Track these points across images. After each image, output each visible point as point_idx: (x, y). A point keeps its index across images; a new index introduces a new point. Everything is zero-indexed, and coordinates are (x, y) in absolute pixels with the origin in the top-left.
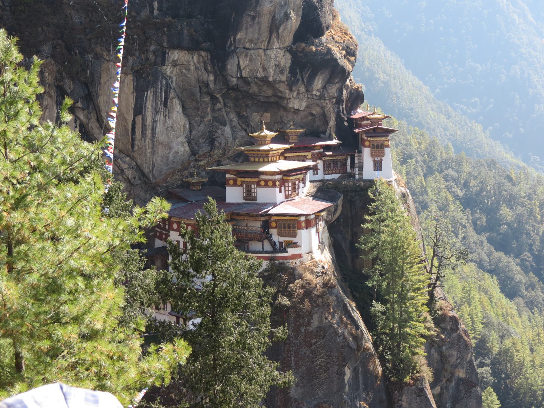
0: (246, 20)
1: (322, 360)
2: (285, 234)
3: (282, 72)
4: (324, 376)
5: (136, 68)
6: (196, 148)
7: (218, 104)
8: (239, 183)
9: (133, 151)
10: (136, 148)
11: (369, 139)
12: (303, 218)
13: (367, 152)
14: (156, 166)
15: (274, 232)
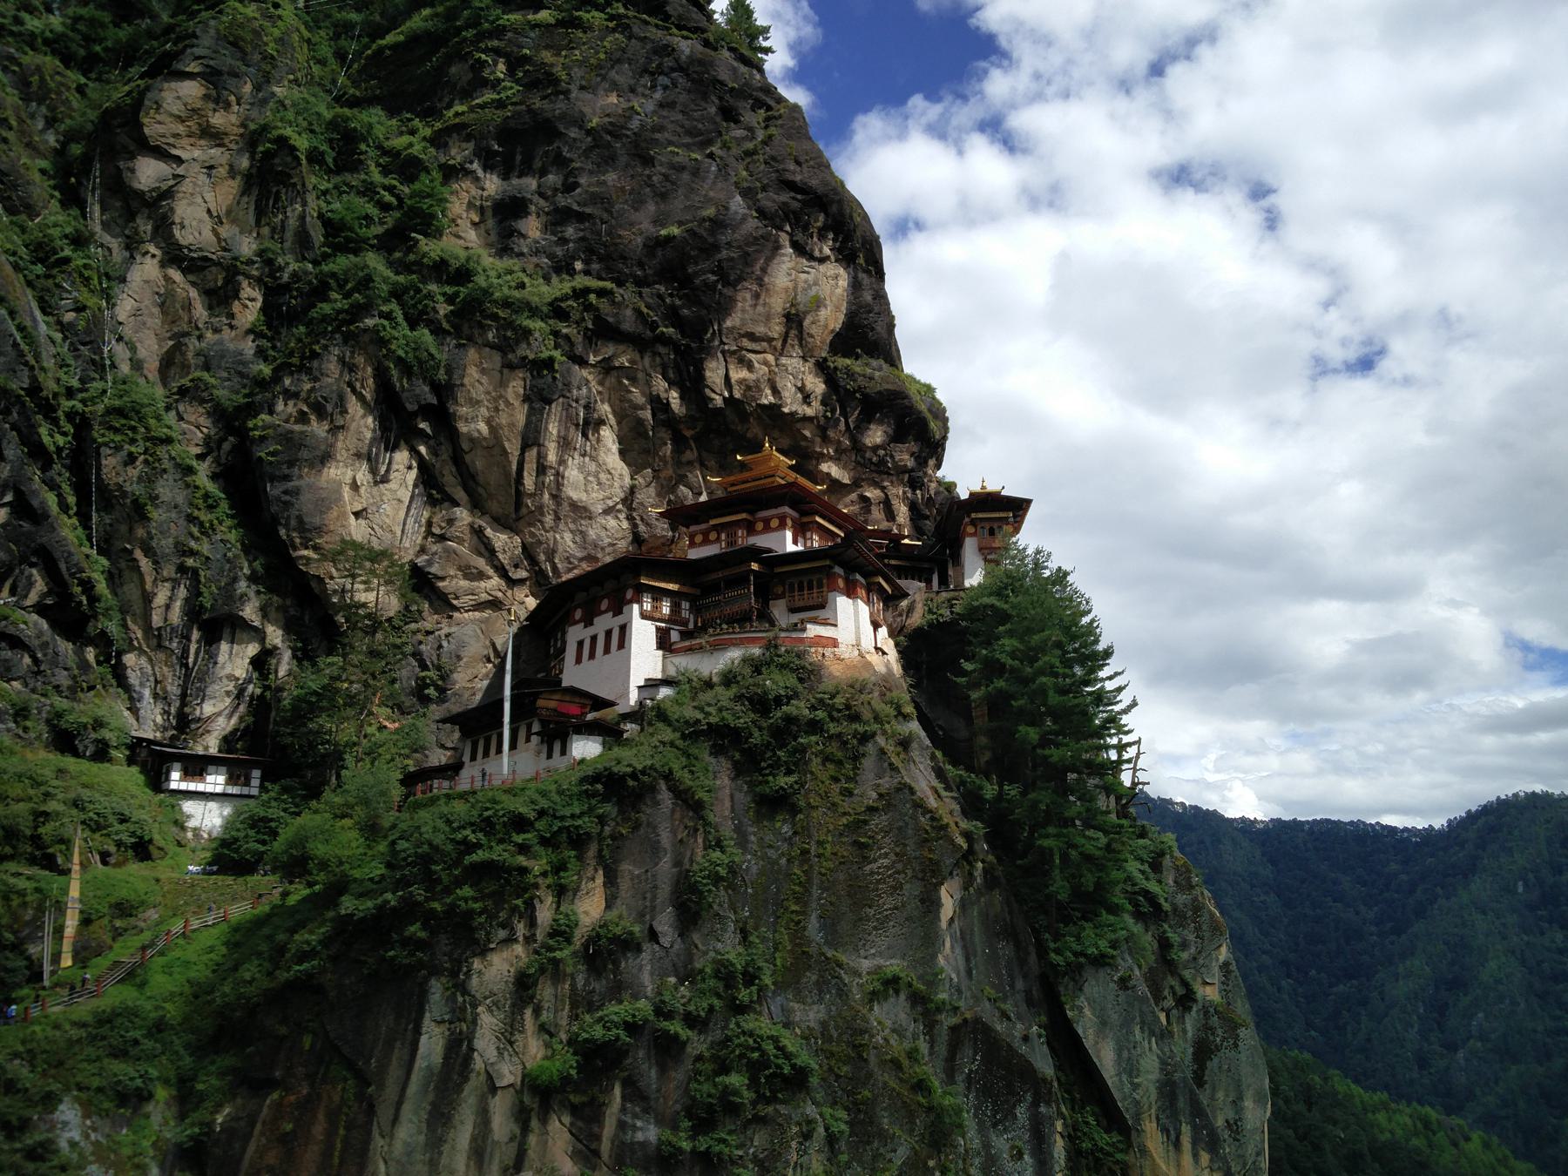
0: (744, 299)
1: (886, 862)
2: (801, 604)
3: (807, 398)
4: (889, 902)
5: (532, 356)
6: (642, 528)
7: (688, 452)
8: (713, 536)
9: (518, 519)
10: (524, 511)
11: (973, 515)
12: (838, 570)
13: (970, 547)
14: (560, 549)
15: (779, 611)
